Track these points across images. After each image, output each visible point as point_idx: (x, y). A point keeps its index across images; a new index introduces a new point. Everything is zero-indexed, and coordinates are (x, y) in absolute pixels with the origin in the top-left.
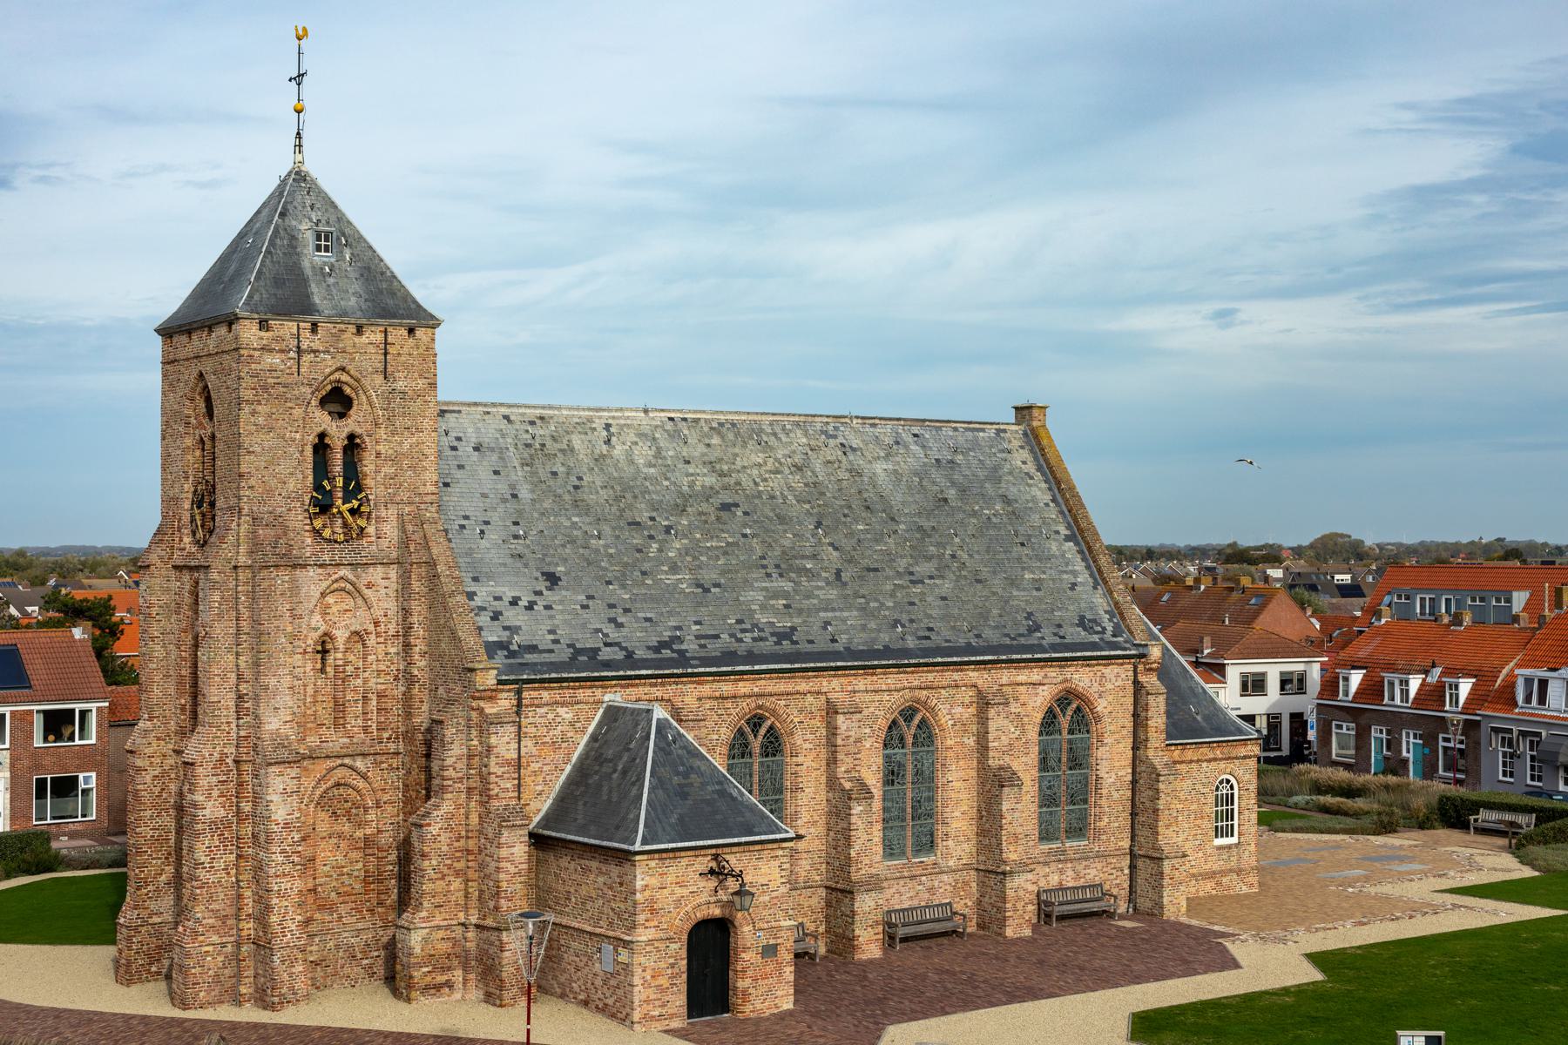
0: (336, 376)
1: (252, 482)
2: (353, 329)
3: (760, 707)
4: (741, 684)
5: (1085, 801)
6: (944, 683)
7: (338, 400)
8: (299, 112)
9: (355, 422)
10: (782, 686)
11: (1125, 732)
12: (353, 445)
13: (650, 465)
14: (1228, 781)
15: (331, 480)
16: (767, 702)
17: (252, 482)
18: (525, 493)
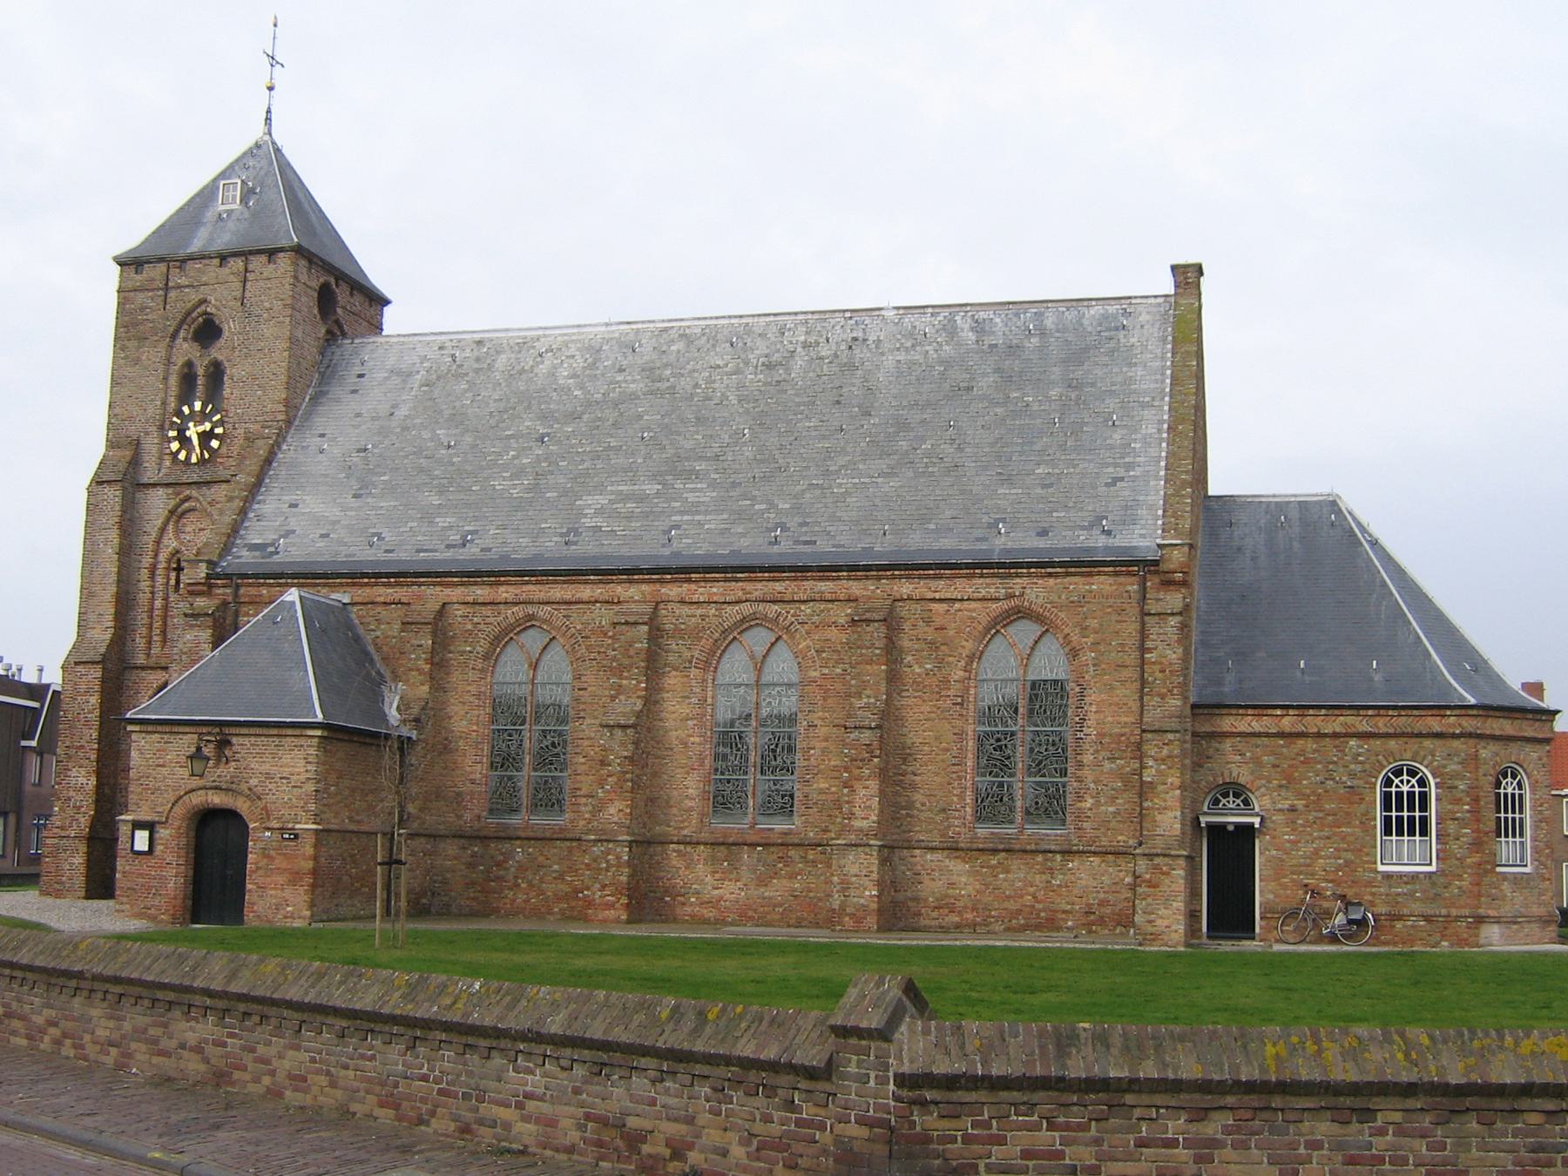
4: (502, 589)
5: (1064, 773)
9: (218, 352)
10: (558, 592)
11: (1126, 673)
12: (216, 373)
13: (574, 376)
14: (1412, 773)
15: (191, 407)
18: (402, 412)
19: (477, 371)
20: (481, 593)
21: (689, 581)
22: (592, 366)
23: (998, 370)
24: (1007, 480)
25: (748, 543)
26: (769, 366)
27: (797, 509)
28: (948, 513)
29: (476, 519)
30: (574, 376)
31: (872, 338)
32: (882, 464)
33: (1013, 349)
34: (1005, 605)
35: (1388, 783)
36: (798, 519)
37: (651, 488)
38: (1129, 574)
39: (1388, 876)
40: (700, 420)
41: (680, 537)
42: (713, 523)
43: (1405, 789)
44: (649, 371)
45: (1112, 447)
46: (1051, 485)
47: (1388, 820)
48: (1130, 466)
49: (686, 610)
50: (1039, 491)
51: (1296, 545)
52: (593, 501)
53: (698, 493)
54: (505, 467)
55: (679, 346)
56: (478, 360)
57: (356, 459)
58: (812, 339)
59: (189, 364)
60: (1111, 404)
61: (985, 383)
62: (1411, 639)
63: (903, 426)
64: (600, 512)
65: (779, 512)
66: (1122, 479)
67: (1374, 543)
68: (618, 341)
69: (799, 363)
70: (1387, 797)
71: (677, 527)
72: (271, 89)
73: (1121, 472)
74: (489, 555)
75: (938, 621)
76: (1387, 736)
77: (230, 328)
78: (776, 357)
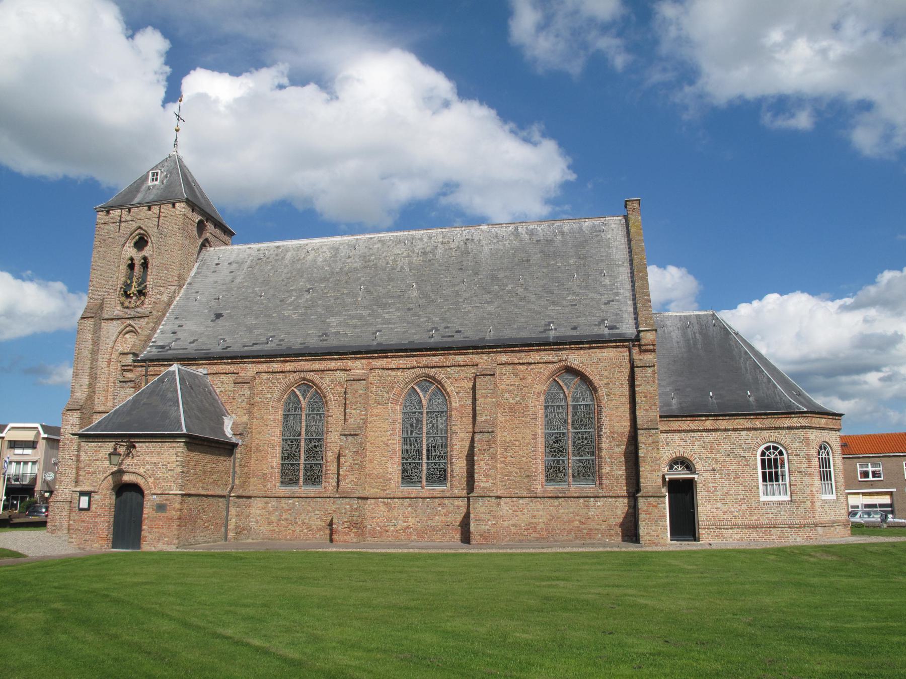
0: (139, 231)
1: (94, 283)
2: (146, 208)
3: (304, 379)
6: (448, 364)
7: (141, 243)
8: (177, 131)
9: (147, 252)
10: (317, 365)
12: (145, 264)
16: (309, 376)
17: (94, 283)
18: (238, 280)
19: (276, 260)
20: (276, 367)
21: (387, 357)
22: (335, 256)
23: (542, 252)
24: (553, 303)
25: (418, 337)
26: (425, 253)
27: (444, 320)
28: (523, 320)
29: (274, 330)
30: (325, 261)
31: (476, 239)
32: (487, 297)
33: (549, 242)
34: (557, 366)
35: (763, 454)
36: (443, 325)
37: (366, 312)
38: (624, 346)
39: (766, 503)
40: (390, 279)
41: (381, 336)
42: (399, 328)
43: (772, 457)
44: (363, 257)
45: (605, 286)
46: (575, 305)
47: (764, 474)
48: (616, 295)
49: (386, 373)
50: (570, 307)
51: (697, 335)
52: (334, 320)
53: (391, 314)
54: (290, 304)
55: (379, 245)
56: (277, 255)
57: (214, 303)
58: (446, 240)
59: (132, 259)
60: (602, 266)
61: (536, 258)
62: (765, 380)
63: (495, 278)
64: (339, 324)
65: (433, 322)
66: (612, 301)
67: (737, 334)
68: (348, 245)
69: (439, 252)
70: (763, 461)
71: (380, 331)
72: (177, 131)
73: (611, 298)
74: (280, 348)
75: (521, 375)
76: (761, 429)
77: (153, 240)
78: (428, 249)
